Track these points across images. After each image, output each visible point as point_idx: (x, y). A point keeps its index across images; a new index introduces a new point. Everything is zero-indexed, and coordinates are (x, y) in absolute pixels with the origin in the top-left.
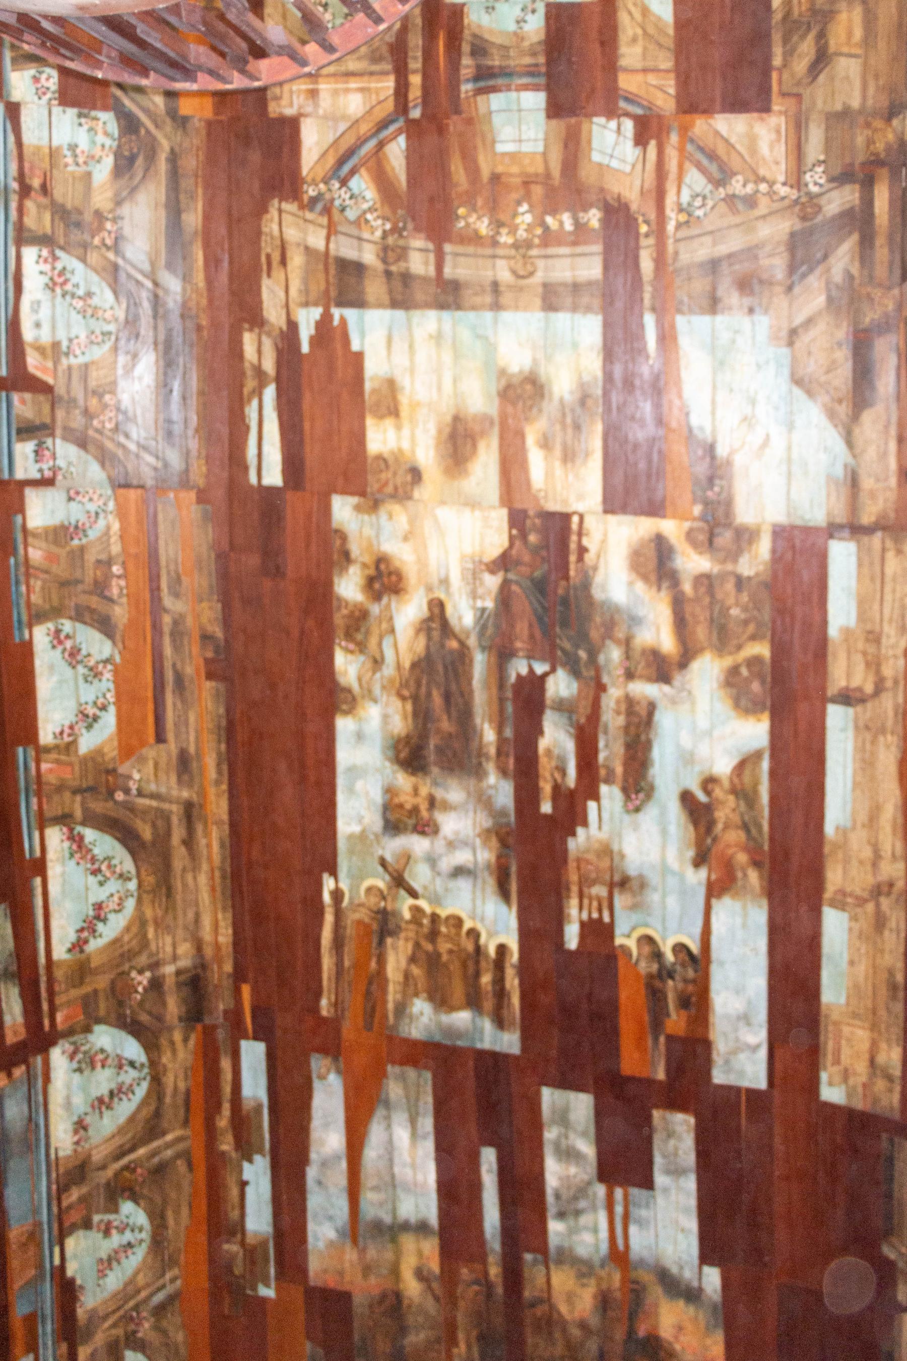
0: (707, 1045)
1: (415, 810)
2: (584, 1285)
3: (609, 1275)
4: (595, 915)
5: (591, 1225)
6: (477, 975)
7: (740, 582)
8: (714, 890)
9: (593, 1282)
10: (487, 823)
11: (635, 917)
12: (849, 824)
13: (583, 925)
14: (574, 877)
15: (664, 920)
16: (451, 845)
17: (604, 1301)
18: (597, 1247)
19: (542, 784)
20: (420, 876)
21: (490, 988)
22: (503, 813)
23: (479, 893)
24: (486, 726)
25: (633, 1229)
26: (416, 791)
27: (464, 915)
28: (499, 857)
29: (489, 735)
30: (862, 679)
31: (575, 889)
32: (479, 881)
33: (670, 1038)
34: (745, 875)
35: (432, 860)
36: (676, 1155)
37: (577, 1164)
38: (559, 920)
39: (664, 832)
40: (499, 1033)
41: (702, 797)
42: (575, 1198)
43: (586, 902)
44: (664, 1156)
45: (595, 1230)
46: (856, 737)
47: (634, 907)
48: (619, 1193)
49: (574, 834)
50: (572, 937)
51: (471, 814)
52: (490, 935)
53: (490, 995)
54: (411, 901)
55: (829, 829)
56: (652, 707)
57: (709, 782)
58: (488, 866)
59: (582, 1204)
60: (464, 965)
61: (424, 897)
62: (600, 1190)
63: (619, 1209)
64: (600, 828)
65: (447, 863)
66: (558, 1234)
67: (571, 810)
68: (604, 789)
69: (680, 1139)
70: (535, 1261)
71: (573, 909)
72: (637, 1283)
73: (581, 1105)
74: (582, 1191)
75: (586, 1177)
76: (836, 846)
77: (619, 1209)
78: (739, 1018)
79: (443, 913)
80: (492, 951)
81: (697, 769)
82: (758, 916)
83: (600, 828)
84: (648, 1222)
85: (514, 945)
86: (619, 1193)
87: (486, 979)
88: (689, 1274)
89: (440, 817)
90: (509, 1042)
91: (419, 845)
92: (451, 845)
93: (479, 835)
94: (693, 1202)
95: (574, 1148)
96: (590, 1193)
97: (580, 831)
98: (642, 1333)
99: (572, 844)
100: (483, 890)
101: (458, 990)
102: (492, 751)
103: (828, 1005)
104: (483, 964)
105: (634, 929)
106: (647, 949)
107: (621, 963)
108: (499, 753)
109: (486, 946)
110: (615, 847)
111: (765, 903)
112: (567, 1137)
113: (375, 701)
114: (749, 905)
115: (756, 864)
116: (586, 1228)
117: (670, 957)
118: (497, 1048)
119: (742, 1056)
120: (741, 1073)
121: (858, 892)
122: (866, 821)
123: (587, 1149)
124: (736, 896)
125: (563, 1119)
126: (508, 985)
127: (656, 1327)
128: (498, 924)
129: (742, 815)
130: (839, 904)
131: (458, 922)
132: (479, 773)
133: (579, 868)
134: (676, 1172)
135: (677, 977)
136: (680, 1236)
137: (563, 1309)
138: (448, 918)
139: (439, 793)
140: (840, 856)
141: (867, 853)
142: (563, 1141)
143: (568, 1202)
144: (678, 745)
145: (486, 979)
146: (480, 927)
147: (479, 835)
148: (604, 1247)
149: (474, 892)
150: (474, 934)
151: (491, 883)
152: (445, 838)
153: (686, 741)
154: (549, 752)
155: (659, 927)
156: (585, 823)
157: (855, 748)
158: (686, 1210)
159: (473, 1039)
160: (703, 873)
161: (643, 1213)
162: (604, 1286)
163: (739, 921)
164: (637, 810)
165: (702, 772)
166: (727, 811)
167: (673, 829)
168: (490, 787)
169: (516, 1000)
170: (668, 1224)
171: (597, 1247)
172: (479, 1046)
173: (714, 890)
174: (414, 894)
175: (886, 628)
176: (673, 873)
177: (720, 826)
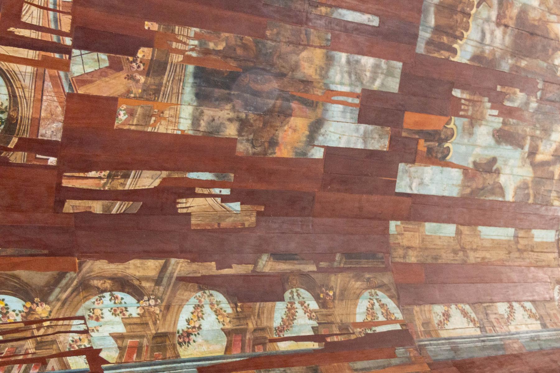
0: (413, 162)
1: (505, 16)
2: (316, 70)
3: (320, 88)
4: (463, 107)
5: (343, 81)
6: (447, 34)
7: (550, 191)
8: (465, 170)
9: (317, 77)
10: (498, 54)
11: (460, 128)
12: (482, 237)
13: (460, 99)
14: (476, 98)
15: (458, 143)
16: (492, 33)
17: (307, 83)
18: (333, 83)
19: (506, 87)
20: (484, 12)
21: (442, 41)
22: (500, 65)
23: (474, 43)
24: (526, 63)
25: (341, 107)
26: (511, 18)
27: (469, 33)
28: (485, 57)
29: (523, 63)
30: (522, 242)
31: (472, 98)
32: (478, 45)
33: (417, 140)
34: (468, 186)
35: (488, 20)
36: (373, 138)
37: (371, 77)
38: (463, 87)
39: (486, 148)
40: (424, 42)
41: (494, 168)
42: (356, 74)
43: (467, 103)
44: (372, 131)
45: (341, 84)
46: (505, 240)
47: (464, 129)
48: (357, 101)
49: (489, 101)
50: (457, 93)
51: (501, 47)
52: (461, 46)
53: (438, 40)
54: (476, 3)
55: (480, 228)
56: (522, 147)
57: (498, 172)
58: (483, 52)
59: (353, 77)
60: (451, 28)
61: (477, 11)
62: (358, 90)
63: (350, 100)
64: (490, 115)
65: (487, 27)
66: (341, 58)
67: (497, 102)
68: (501, 119)
69: (379, 142)
70: (327, 40)
71: (466, 96)
72: (317, 106)
73: (393, 85)
74: (359, 79)
75: (364, 82)
76: (475, 230)
77: (350, 100)
78: (422, 179)
79: (470, 20)
80: (455, 46)
81: (503, 167)
82: (454, 192)
83: (490, 115)
84: (344, 118)
85: (456, 59)
86: (357, 101)
87: (445, 39)
88: (320, 140)
89: (502, 28)
90: (421, 48)
91: (494, 15)
92: (492, 33)
93: (494, 49)
94: (352, 146)
95: (377, 77)
96: (358, 83)
97: (489, 105)
98: (294, 105)
99: (486, 99)
100: (476, 47)
101: (443, 22)
102: (518, 64)
103: (424, 226)
104: (451, 39)
105: (457, 127)
106: (449, 133)
107: (445, 119)
108: (517, 66)
109: (456, 43)
110: (483, 122)
111: (459, 196)
112: (382, 73)
113: (540, 5)
114: (459, 188)
115: (472, 192)
116: (342, 77)
117: (446, 145)
118: (419, 39)
119: (408, 179)
120: (402, 179)
121: (463, 241)
122: (484, 245)
123: (376, 86)
124: (463, 181)
125: (389, 73)
126: (442, 52)
127: (296, 116)
128: (464, 53)
129: (487, 187)
130: (459, 233)
131: (467, 30)
132: (513, 55)
133: (478, 101)
134: (365, 138)
135: (438, 148)
136: (338, 136)
137: (304, 54)
138: (468, 23)
139: (509, 31)
140: (472, 233)
141: (475, 247)
142: (380, 71)
143: (355, 68)
144: (510, 158)
145: (445, 39)
146: (464, 40)
147: (494, 49)
148: (333, 87)
149: (476, 41)
150: (461, 37)
151: (478, 52)
152: (495, 30)
153: (511, 162)
154: (515, 93)
155: (456, 141)
156: (492, 108)
157: (502, 240)
158: (349, 142)
159: (424, 25)
160: (471, 166)
161: (348, 115)
162: (315, 84)
163: (455, 182)
164: (493, 136)
165: (501, 168)
166: (490, 179)
167: (486, 152)
168: (508, 61)
169: (436, 55)
170: (343, 131)
171: (333, 83)
172: (420, 28)
173: (465, 170)
174: (478, 6)
175: (536, 254)
176: (473, 150)
177: (485, 176)
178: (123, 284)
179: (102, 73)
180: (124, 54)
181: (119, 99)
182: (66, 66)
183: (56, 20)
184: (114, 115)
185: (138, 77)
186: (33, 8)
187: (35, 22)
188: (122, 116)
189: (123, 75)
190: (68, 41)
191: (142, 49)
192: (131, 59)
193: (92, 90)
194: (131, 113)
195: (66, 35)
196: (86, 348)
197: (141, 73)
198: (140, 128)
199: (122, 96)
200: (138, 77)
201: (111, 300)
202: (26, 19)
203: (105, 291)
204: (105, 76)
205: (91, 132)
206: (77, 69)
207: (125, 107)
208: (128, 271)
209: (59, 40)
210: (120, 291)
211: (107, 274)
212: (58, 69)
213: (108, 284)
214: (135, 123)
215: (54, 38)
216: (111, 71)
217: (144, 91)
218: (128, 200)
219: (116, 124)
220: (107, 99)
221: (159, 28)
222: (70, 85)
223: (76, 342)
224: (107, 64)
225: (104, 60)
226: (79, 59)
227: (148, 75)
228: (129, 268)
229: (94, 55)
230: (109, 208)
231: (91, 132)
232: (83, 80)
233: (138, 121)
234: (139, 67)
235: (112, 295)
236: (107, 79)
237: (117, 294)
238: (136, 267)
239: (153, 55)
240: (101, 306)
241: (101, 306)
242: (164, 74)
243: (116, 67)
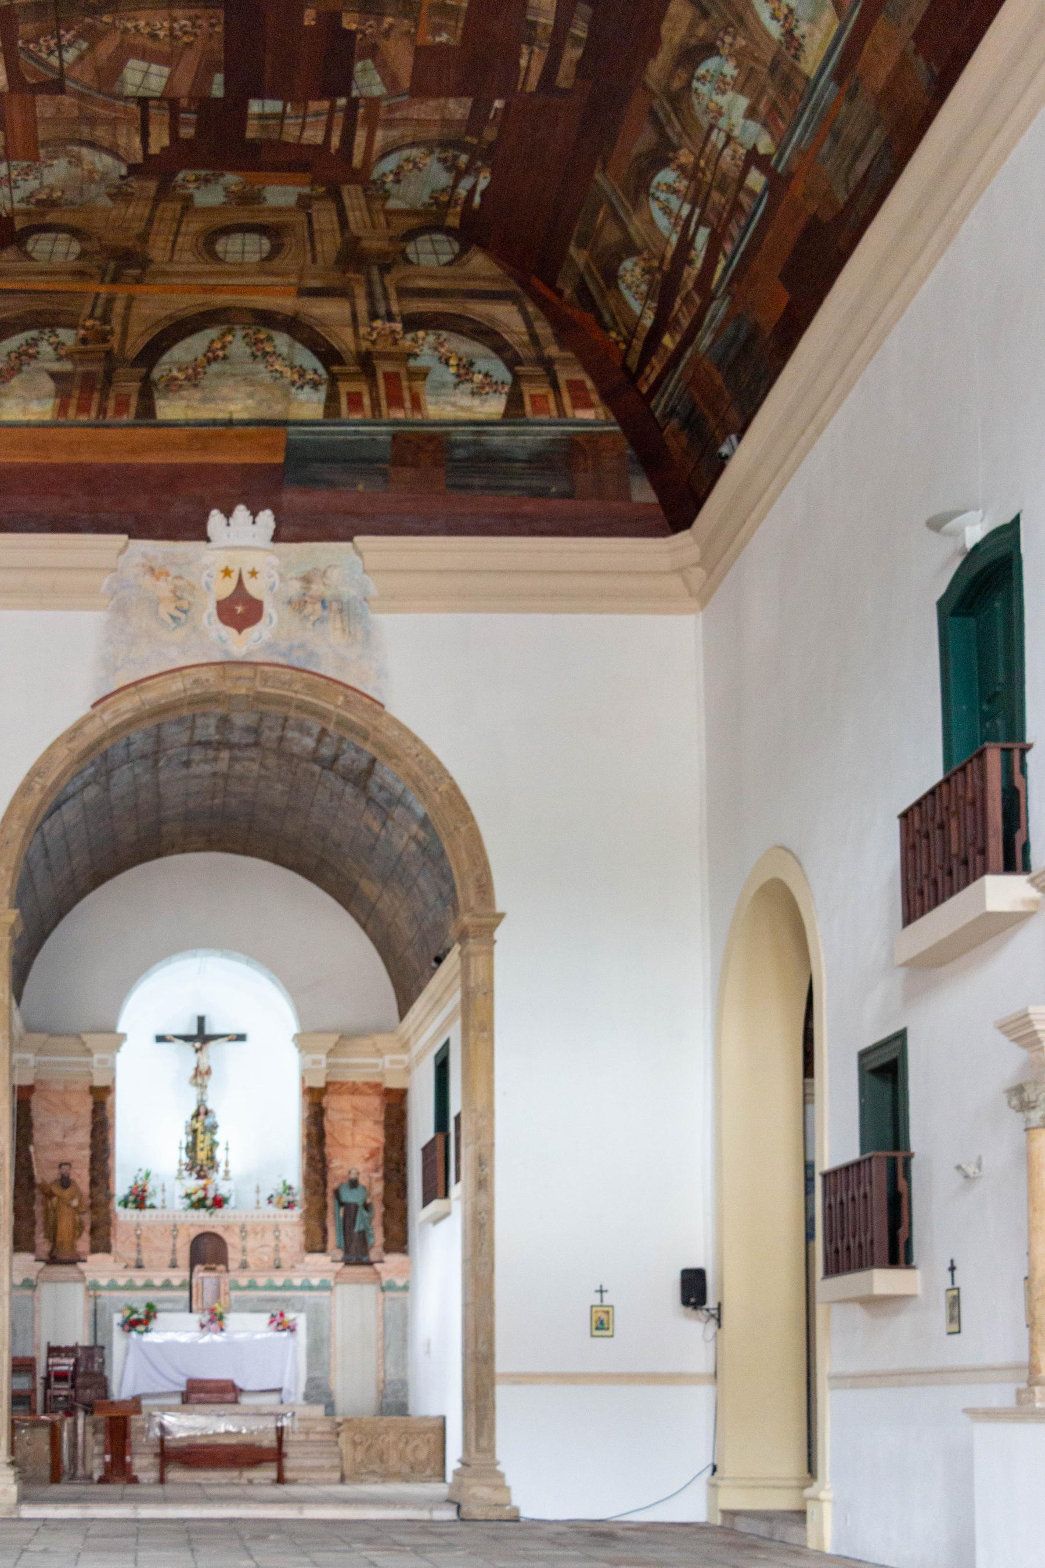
179: (382, 67)
181: (420, 42)
188: (444, 38)
207: (430, 38)
224: (369, 61)
230: (577, 41)
236: (390, 60)
240: (706, 98)
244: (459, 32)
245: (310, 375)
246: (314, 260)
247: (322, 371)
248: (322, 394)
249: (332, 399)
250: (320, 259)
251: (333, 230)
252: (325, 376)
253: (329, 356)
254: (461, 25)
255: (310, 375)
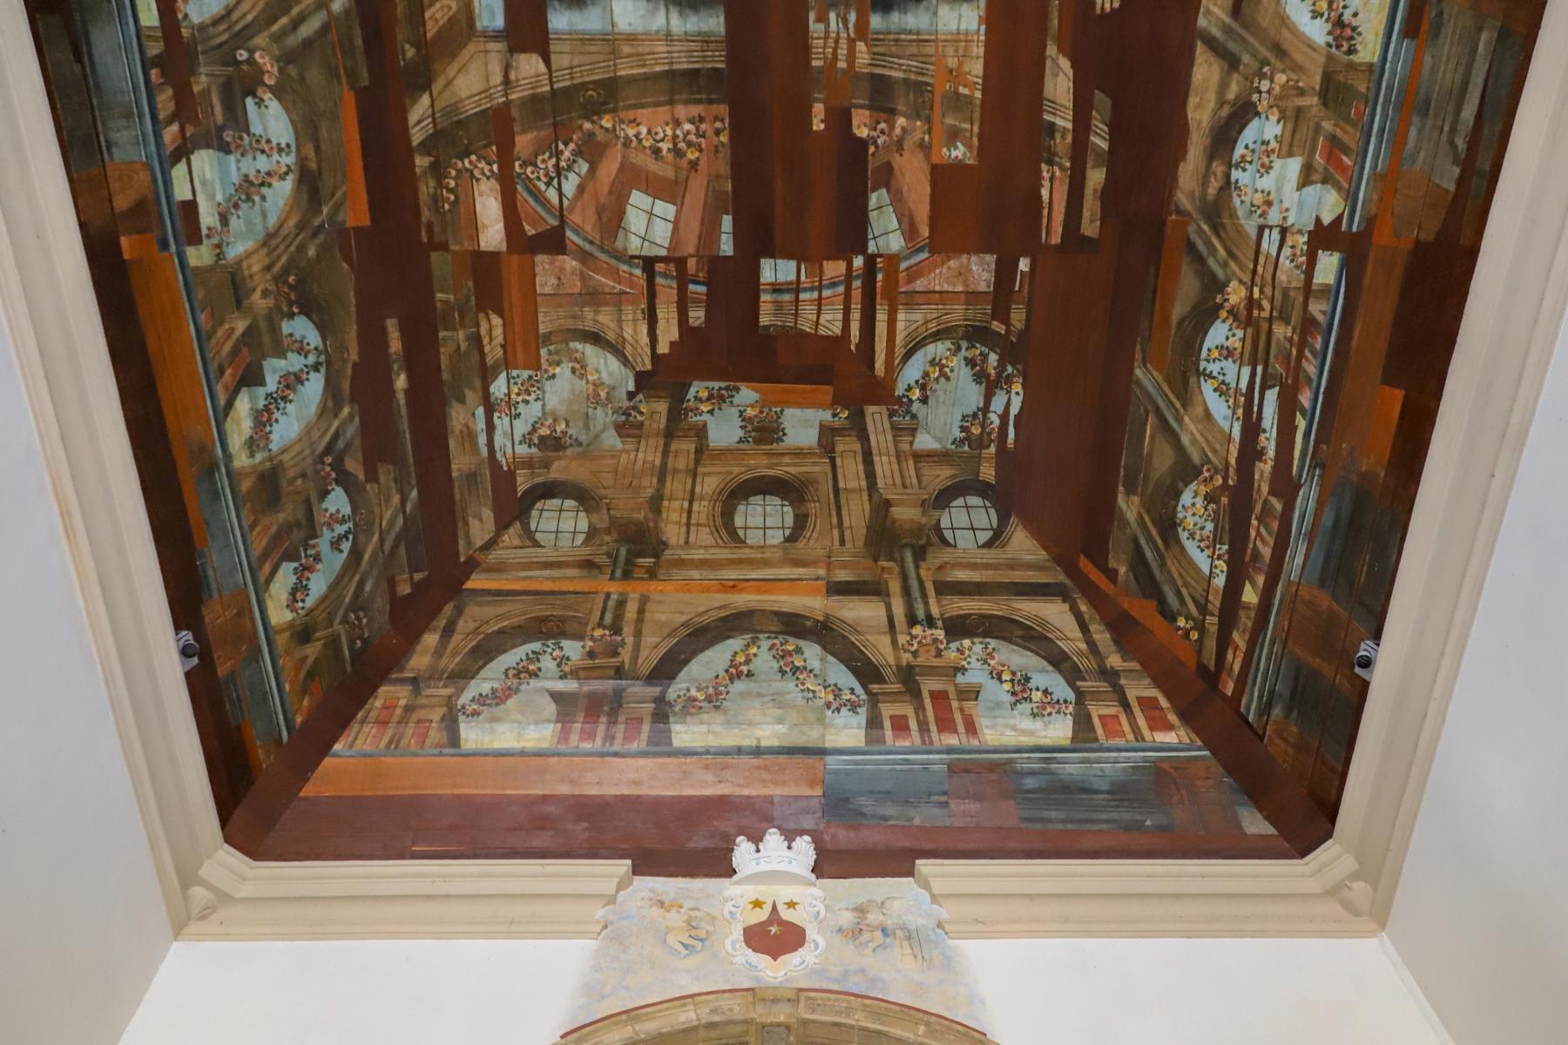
178: (1224, 136)
179: (897, 200)
180: (865, 161)
181: (935, 160)
182: (893, 259)
183: (833, 285)
184: (958, 166)
185: (898, 131)
186: (822, 321)
187: (840, 316)
188: (959, 152)
189: (897, 161)
190: (858, 262)
191: (856, 131)
192: (872, 149)
193: (922, 212)
194: (954, 136)
195: (850, 264)
196: (1308, 243)
197: (892, 126)
198: (977, 115)
199: (928, 157)
200: (898, 131)
201: (1244, 170)
202: (837, 329)
203: (1228, 176)
204: (900, 191)
205: (985, 207)
206: (895, 243)
208: (1204, 124)
209: (858, 277)
210: (1233, 149)
211: (1202, 169)
212: (897, 271)
213: (1218, 168)
214: (967, 126)
215: (857, 284)
216: (893, 183)
217: (918, 117)
218: (1090, 118)
219: (971, 162)
220: (934, 183)
221: (818, 100)
222: (920, 250)
223: (1294, 255)
225: (879, 198)
226: (881, 241)
227: (892, 112)
228: (1200, 122)
229: (873, 215)
231: (985, 207)
232: (910, 231)
233: (965, 120)
234: (882, 132)
235: (1237, 166)
236: (905, 189)
237: (1239, 151)
238: (1199, 106)
239: (862, 107)
241: (1249, 190)
242: (889, 77)
243: (886, 177)
244: (975, 140)
245: (847, 696)
246: (842, 543)
247: (859, 690)
248: (862, 716)
249: (874, 723)
250: (849, 545)
251: (860, 490)
252: (864, 697)
253: (867, 672)
254: (976, 129)
255: (847, 696)
